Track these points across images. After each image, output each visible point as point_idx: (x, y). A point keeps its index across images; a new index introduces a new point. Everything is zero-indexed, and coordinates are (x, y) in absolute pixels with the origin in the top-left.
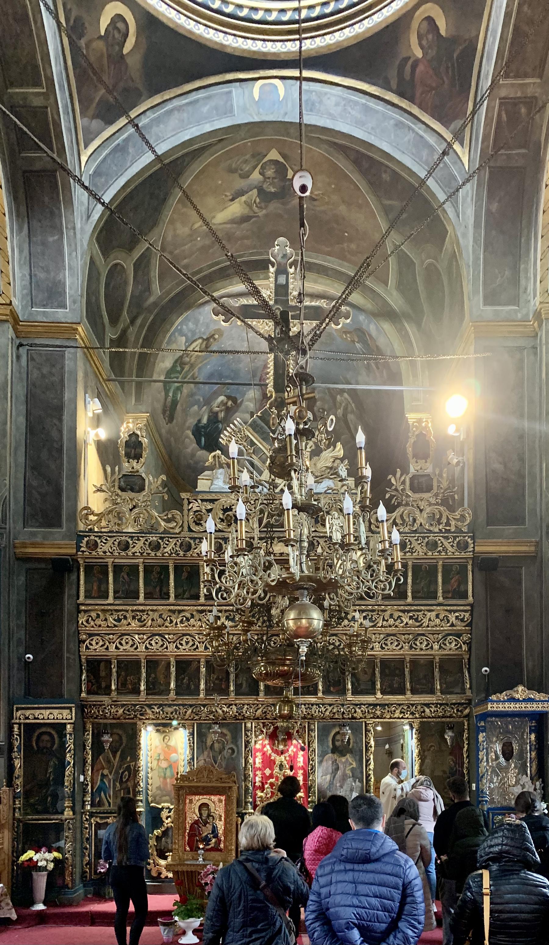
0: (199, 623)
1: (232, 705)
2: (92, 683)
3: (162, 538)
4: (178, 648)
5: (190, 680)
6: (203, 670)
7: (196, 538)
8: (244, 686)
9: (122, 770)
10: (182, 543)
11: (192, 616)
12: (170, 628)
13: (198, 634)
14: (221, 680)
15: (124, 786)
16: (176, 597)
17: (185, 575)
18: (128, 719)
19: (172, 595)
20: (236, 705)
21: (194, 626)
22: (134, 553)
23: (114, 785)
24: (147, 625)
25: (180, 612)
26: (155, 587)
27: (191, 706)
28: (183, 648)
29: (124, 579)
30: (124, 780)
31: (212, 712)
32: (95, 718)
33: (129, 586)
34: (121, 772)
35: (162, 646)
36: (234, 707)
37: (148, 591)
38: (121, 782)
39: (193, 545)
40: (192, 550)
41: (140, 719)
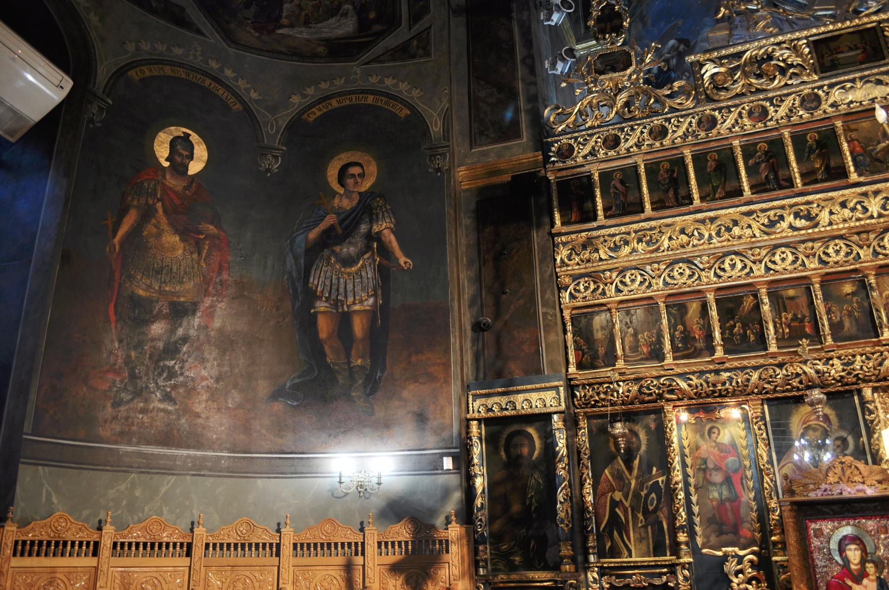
0: (748, 232)
1: (831, 359)
2: (583, 351)
3: (668, 120)
4: (719, 277)
5: (745, 326)
6: (766, 308)
7: (722, 108)
8: (847, 324)
9: (645, 492)
10: (700, 119)
11: (736, 223)
12: (701, 247)
13: (751, 249)
14: (802, 321)
15: (652, 518)
16: (702, 199)
17: (711, 164)
18: (649, 402)
19: (696, 196)
20: (839, 358)
21: (740, 237)
22: (628, 150)
23: (635, 517)
24: (662, 249)
25: (712, 220)
26: (667, 191)
27: (755, 368)
28: (728, 274)
29: (617, 189)
30: (651, 508)
31: (798, 375)
32: (593, 406)
33: (626, 196)
34: (643, 494)
35: (690, 276)
36: (836, 361)
37: (656, 199)
38: (646, 512)
39: (719, 117)
40: (718, 126)
41: (668, 400)
